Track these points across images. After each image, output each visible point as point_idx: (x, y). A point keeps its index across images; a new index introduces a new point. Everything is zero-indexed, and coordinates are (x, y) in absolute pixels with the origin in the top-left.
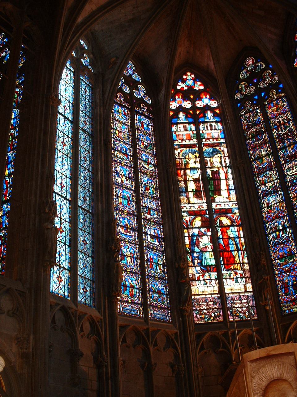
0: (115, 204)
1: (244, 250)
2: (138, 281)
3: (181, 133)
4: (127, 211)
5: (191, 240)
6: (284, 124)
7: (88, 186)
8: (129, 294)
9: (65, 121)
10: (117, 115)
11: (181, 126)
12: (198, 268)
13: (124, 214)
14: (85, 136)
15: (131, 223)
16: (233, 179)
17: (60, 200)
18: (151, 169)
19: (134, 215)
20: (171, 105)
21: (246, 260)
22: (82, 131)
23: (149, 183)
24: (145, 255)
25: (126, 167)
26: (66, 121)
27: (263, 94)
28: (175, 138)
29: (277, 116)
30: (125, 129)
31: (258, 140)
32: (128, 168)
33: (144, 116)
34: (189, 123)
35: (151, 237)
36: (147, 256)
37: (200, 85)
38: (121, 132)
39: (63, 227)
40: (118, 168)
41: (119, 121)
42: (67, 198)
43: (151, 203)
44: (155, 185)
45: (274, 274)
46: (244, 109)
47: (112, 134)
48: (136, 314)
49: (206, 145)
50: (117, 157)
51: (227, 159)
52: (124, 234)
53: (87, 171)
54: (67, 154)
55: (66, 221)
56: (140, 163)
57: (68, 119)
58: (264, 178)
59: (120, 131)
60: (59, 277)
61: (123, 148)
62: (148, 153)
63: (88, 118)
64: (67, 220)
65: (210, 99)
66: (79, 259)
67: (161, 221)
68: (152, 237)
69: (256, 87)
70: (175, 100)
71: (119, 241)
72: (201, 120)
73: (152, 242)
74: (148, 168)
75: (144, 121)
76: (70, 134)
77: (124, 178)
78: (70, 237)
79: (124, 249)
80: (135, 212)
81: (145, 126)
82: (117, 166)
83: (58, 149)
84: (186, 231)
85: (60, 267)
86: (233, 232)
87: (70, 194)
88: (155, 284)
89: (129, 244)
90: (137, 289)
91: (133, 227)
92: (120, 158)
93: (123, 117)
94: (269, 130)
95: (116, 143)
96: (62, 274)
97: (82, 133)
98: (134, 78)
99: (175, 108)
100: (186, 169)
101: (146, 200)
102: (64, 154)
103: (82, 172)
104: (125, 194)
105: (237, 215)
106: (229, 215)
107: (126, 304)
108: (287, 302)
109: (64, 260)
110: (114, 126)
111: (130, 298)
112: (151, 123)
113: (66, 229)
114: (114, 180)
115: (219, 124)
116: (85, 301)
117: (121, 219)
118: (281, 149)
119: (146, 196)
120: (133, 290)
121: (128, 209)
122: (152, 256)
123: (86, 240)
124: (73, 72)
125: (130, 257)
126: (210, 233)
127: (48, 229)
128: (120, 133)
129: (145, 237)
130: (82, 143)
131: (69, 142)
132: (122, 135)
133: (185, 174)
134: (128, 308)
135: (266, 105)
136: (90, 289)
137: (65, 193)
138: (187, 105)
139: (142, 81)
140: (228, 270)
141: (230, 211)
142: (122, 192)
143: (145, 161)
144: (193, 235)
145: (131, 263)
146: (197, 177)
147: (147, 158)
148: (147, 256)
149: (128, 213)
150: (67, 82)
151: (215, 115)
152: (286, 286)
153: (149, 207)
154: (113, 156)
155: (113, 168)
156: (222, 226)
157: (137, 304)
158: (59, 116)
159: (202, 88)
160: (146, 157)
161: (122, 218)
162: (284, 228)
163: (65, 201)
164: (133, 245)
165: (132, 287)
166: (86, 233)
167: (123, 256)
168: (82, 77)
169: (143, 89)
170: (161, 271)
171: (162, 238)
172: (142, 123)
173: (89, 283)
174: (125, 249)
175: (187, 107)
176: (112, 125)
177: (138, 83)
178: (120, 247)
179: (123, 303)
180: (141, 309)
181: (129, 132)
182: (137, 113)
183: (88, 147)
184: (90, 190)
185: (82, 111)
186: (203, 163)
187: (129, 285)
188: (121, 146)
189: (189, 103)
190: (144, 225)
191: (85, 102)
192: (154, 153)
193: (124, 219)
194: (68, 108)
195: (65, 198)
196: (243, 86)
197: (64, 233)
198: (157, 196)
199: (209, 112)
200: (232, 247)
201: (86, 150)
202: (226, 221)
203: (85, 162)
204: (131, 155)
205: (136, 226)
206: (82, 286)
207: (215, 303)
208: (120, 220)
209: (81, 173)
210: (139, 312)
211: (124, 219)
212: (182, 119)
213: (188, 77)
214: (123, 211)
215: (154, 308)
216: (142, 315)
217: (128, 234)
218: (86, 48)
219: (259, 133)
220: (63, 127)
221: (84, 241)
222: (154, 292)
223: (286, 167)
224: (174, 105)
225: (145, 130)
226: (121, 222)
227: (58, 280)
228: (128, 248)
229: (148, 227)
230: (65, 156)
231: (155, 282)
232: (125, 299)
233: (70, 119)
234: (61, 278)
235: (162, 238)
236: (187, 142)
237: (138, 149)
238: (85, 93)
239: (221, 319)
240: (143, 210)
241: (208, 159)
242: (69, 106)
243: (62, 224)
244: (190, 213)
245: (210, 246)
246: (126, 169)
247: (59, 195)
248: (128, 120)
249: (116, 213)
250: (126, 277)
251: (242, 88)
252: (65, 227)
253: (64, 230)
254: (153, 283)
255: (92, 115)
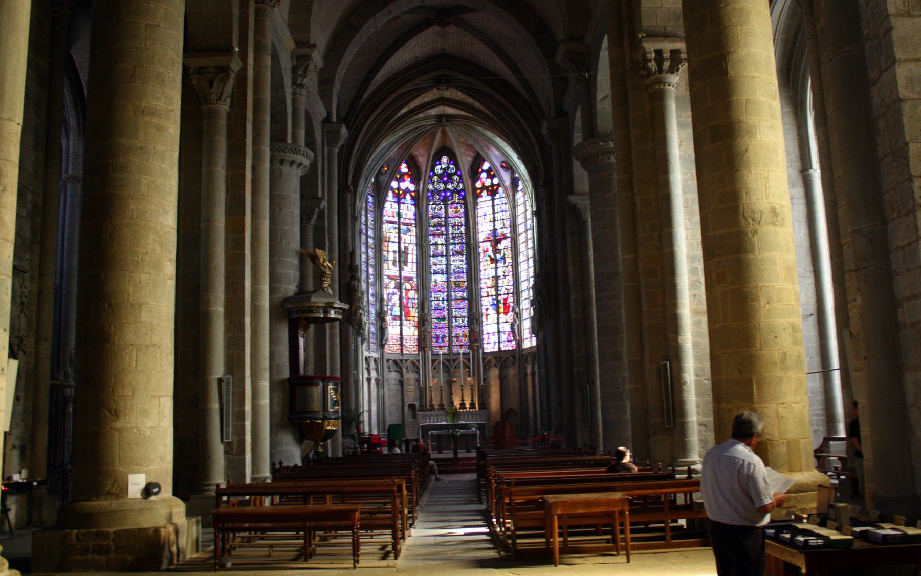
1: (417, 308)
5: (388, 297)
6: (458, 226)
12: (390, 317)
16: (417, 255)
21: (416, 315)
27: (449, 194)
29: (454, 217)
31: (438, 230)
34: (395, 202)
37: (406, 167)
45: (432, 328)
46: (433, 200)
49: (404, 224)
51: (415, 237)
58: (436, 261)
65: (412, 182)
69: (446, 186)
72: (402, 201)
84: (385, 289)
86: (412, 294)
94: (446, 225)
100: (389, 241)
105: (415, 283)
106: (411, 282)
108: (436, 347)
115: (413, 206)
118: (452, 244)
126: (399, 294)
133: (388, 246)
135: (449, 204)
138: (394, 184)
140: (406, 320)
141: (411, 279)
144: (388, 294)
146: (394, 250)
151: (413, 198)
152: (437, 337)
156: (406, 289)
159: (406, 170)
162: (443, 300)
186: (399, 238)
196: (436, 180)
199: (408, 195)
200: (410, 305)
202: (409, 287)
207: (397, 341)
219: (439, 225)
223: (452, 258)
236: (391, 219)
239: (399, 351)
241: (402, 236)
244: (389, 277)
245: (398, 303)
251: (434, 181)
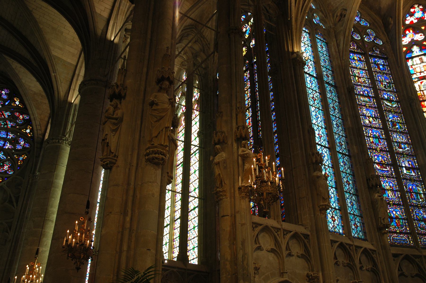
0: (367, 145)
2: (402, 212)
3: (418, 65)
4: (379, 148)
7: (341, 132)
8: (396, 224)
9: (311, 78)
10: (353, 63)
11: (416, 60)
13: (377, 152)
14: (330, 88)
15: (385, 159)
17: (320, 149)
18: (394, 106)
19: (386, 151)
20: (403, 41)
22: (327, 84)
23: (394, 119)
24: (404, 187)
25: (371, 108)
26: (312, 78)
28: (412, 72)
30: (363, 74)
32: (373, 109)
33: (378, 58)
35: (406, 169)
36: (406, 187)
38: (360, 78)
39: (327, 173)
40: (364, 111)
41: (356, 68)
42: (326, 146)
43: (400, 137)
44: (400, 120)
47: (353, 81)
48: (406, 243)
50: (361, 101)
52: (380, 170)
53: (338, 119)
54: (319, 107)
55: (329, 167)
56: (383, 103)
57: (313, 76)
59: (359, 77)
60: (332, 217)
61: (364, 91)
62: (389, 91)
63: (329, 71)
64: (330, 166)
66: (346, 198)
67: (413, 152)
68: (407, 169)
70: (405, 36)
71: (378, 177)
73: (409, 174)
74: (390, 105)
75: (379, 63)
76: (317, 89)
77: (371, 119)
78: (335, 180)
79: (383, 184)
80: (387, 148)
81: (381, 67)
82: (363, 109)
83: (310, 105)
85: (332, 208)
87: (328, 142)
88: (419, 213)
89: (387, 179)
90: (403, 219)
91: (388, 162)
92: (364, 101)
93: (359, 63)
95: (358, 89)
96: (335, 214)
97: (327, 85)
98: (362, 24)
99: (407, 43)
101: (395, 136)
102: (316, 108)
103: (334, 121)
104: (375, 133)
107: (395, 235)
109: (334, 201)
110: (352, 73)
111: (397, 228)
112: (386, 63)
113: (331, 174)
114: (362, 122)
116: (358, 235)
117: (376, 157)
119: (394, 131)
120: (399, 220)
121: (380, 147)
122: (411, 187)
123: (349, 180)
124: (308, 32)
125: (390, 190)
127: (318, 177)
128: (359, 79)
129: (401, 170)
130: (329, 95)
131: (318, 97)
132: (362, 80)
134: (398, 238)
136: (360, 224)
137: (324, 142)
139: (370, 25)
142: (372, 132)
143: (387, 100)
145: (392, 196)
147: (388, 96)
148: (406, 187)
149: (381, 150)
150: (305, 43)
153: (399, 141)
154: (357, 101)
155: (360, 111)
157: (405, 233)
158: (305, 75)
160: (387, 95)
161: (376, 155)
163: (325, 149)
164: (391, 179)
165: (398, 218)
166: (347, 174)
167: (384, 190)
168: (317, 35)
169: (372, 32)
170: (423, 200)
171: (417, 169)
172: (378, 65)
173: (358, 219)
174: (384, 184)
175: (419, 40)
176: (351, 72)
177: (365, 28)
178: (380, 181)
179: (392, 234)
180: (410, 238)
181: (367, 76)
182: (371, 56)
183: (335, 97)
184: (344, 135)
185: (323, 66)
187: (394, 216)
188: (363, 90)
189: (421, 35)
190: (398, 158)
191: (324, 57)
192: (394, 90)
193: (378, 157)
194: (311, 66)
195: (325, 147)
197: (329, 177)
198: (405, 129)
201: (333, 100)
203: (335, 111)
204: (373, 96)
205: (390, 161)
206: (353, 223)
208: (374, 157)
209: (333, 122)
210: (409, 241)
211: (378, 157)
212: (417, 52)
213: (415, 10)
214: (376, 150)
215: (423, 237)
216: (412, 243)
217: (384, 169)
218: (314, 7)
220: (310, 84)
221: (347, 181)
222: (419, 220)
224: (406, 41)
225: (382, 71)
226: (376, 159)
227: (333, 220)
228: (387, 183)
229: (402, 160)
230: (317, 110)
231: (419, 211)
232: (394, 229)
233: (315, 75)
234: (334, 217)
235: (417, 169)
237: (379, 89)
238: (322, 49)
240: (394, 146)
242: (311, 64)
243: (327, 170)
246: (371, 110)
247: (319, 145)
248: (364, 64)
249: (370, 152)
250: (390, 210)
252: (330, 172)
253: (329, 174)
254: (417, 213)
255: (332, 67)
